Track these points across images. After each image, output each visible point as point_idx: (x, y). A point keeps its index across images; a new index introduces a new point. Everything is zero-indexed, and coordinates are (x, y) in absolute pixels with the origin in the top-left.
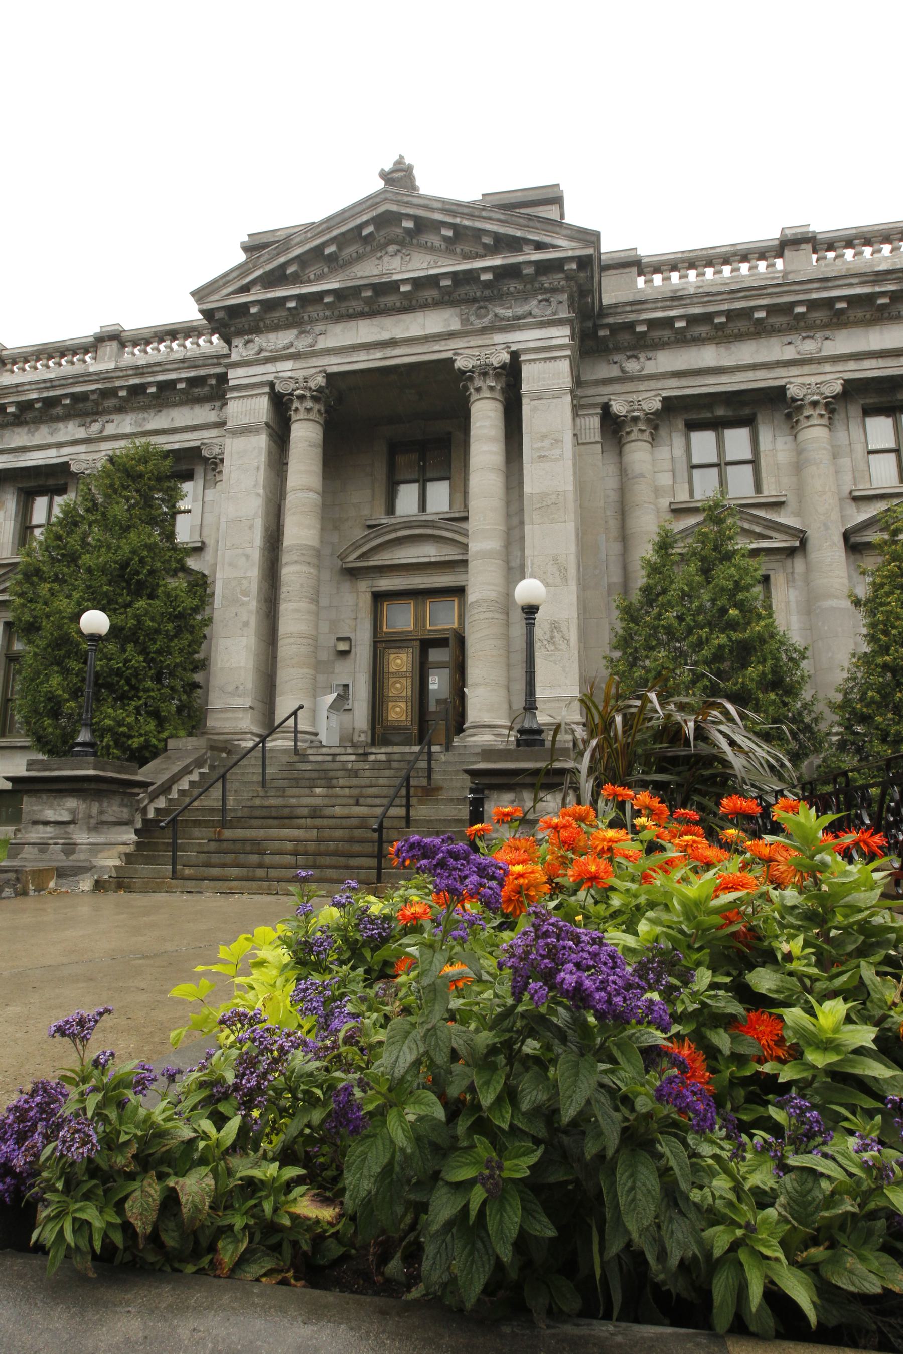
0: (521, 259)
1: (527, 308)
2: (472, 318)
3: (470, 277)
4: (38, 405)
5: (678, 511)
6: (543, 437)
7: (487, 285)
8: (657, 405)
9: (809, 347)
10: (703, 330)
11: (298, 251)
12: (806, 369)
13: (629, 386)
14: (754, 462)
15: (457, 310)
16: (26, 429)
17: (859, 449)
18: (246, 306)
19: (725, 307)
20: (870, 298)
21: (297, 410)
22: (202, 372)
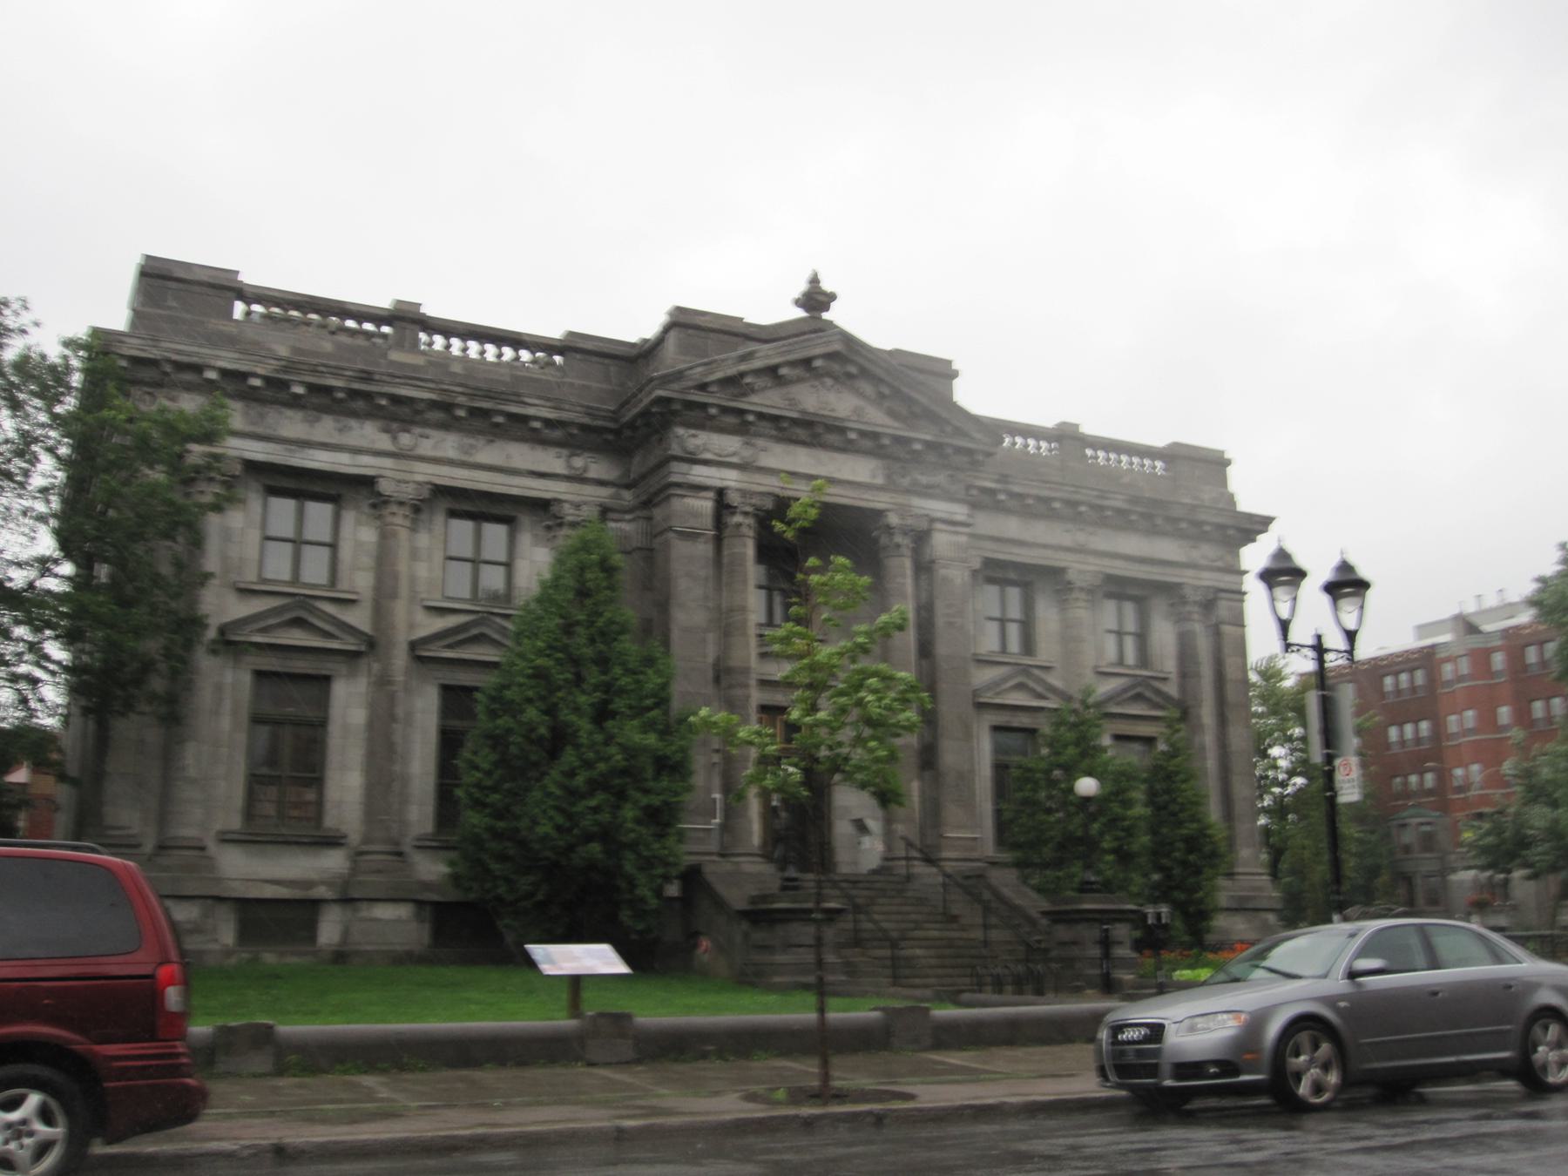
4: (340, 395)
7: (915, 452)
9: (1081, 538)
11: (757, 364)
18: (704, 406)
19: (1034, 492)
22: (565, 416)
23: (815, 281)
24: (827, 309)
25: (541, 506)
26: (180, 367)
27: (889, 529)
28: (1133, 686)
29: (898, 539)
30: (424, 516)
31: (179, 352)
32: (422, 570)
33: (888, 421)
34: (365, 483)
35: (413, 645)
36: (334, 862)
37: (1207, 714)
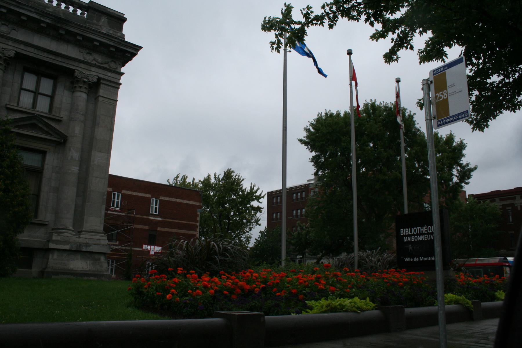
17: (17, 86)
20: (38, 21)
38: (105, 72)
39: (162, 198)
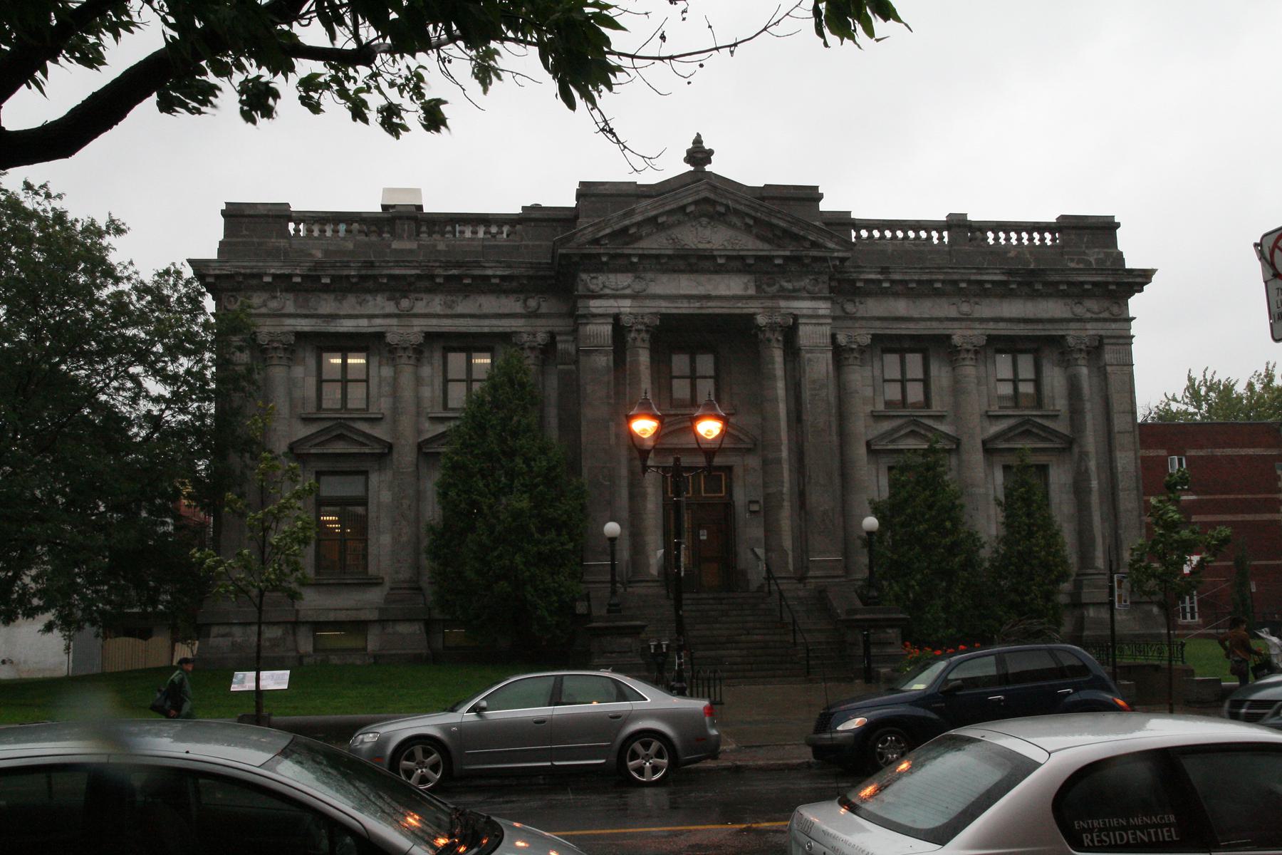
0: (804, 253)
1: (802, 284)
2: (765, 286)
3: (769, 259)
4: (354, 280)
5: (877, 417)
6: (814, 382)
8: (866, 340)
9: (965, 308)
10: (899, 288)
11: (639, 218)
12: (964, 324)
13: (850, 323)
14: (926, 382)
15: (751, 277)
16: (333, 296)
17: (992, 380)
18: (599, 255)
19: (916, 278)
21: (635, 339)
22: (516, 272)
23: (698, 141)
24: (710, 162)
25: (506, 337)
26: (245, 275)
27: (759, 328)
28: (1021, 424)
29: (768, 335)
30: (426, 354)
31: (244, 267)
32: (426, 392)
33: (760, 245)
34: (380, 336)
35: (420, 446)
36: (375, 596)
37: (1091, 441)
38: (1107, 325)
39: (1192, 453)
